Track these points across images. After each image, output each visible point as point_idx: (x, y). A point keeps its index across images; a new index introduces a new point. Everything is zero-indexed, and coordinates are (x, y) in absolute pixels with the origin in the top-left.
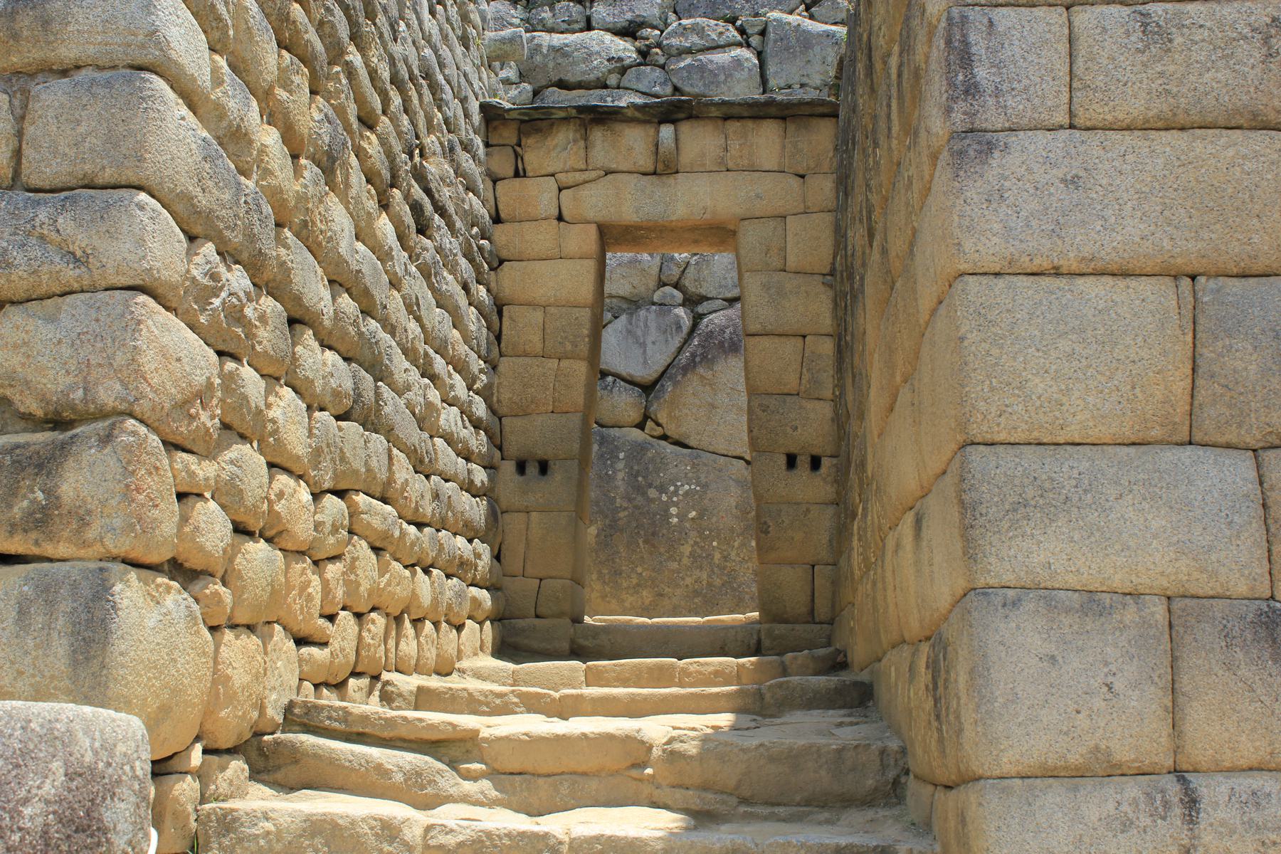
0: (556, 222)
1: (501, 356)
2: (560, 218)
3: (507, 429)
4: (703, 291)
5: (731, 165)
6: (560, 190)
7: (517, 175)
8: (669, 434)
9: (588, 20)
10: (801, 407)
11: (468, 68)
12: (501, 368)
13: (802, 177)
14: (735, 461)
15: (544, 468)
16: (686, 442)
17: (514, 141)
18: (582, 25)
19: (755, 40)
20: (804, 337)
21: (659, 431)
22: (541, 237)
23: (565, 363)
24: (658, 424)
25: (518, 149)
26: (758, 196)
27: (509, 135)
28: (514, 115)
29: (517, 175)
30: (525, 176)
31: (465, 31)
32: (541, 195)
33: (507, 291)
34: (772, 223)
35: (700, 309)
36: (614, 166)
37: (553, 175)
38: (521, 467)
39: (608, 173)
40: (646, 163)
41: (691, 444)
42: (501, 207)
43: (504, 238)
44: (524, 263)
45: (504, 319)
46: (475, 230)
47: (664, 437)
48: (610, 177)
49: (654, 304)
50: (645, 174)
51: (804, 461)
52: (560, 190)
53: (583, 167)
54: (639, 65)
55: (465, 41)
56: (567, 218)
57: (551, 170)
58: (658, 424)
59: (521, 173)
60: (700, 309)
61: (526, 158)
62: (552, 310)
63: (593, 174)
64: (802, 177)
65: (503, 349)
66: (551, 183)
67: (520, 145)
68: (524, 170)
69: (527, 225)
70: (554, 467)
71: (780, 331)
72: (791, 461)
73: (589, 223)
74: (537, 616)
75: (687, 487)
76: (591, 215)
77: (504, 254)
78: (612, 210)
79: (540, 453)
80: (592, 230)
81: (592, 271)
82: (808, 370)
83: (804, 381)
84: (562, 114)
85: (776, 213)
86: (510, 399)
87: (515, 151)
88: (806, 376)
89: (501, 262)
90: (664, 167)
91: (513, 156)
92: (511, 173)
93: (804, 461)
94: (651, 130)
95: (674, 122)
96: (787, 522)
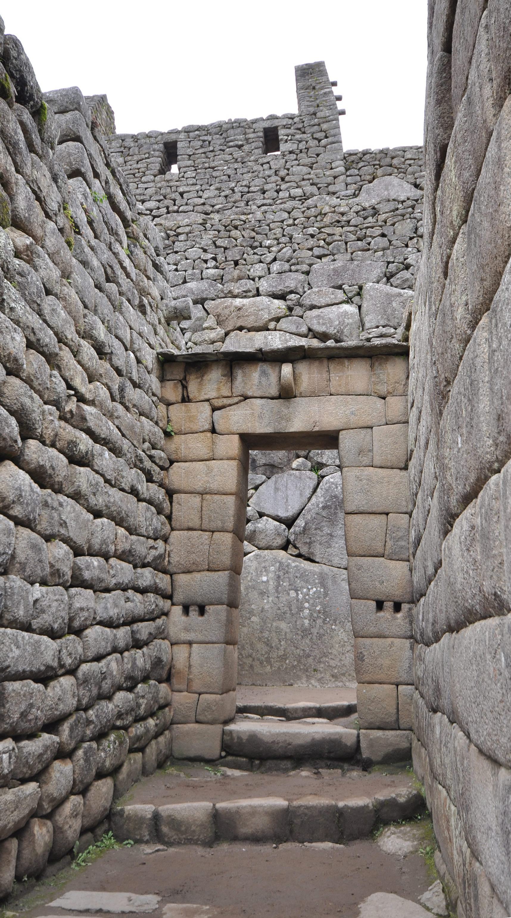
1: (172, 529)
2: (213, 431)
5: (333, 391)
9: (258, 289)
11: (146, 329)
12: (171, 540)
15: (202, 611)
18: (254, 292)
20: (387, 514)
21: (296, 552)
22: (197, 445)
25: (184, 382)
27: (177, 373)
28: (180, 359)
31: (141, 301)
32: (202, 414)
33: (176, 483)
34: (363, 431)
38: (186, 610)
39: (246, 398)
40: (274, 391)
41: (317, 560)
44: (187, 464)
45: (173, 504)
46: (147, 444)
47: (299, 556)
50: (272, 398)
51: (389, 605)
53: (230, 395)
54: (287, 316)
55: (142, 309)
56: (218, 431)
59: (186, 399)
61: (189, 389)
63: (236, 400)
64: (384, 398)
66: (206, 407)
68: (188, 397)
70: (209, 609)
71: (370, 510)
72: (380, 606)
74: (197, 722)
75: (315, 589)
76: (235, 429)
77: (173, 457)
78: (249, 425)
79: (199, 600)
80: (236, 439)
83: (387, 548)
85: (365, 425)
86: (178, 562)
89: (172, 462)
90: (286, 394)
93: (389, 605)
95: (292, 362)
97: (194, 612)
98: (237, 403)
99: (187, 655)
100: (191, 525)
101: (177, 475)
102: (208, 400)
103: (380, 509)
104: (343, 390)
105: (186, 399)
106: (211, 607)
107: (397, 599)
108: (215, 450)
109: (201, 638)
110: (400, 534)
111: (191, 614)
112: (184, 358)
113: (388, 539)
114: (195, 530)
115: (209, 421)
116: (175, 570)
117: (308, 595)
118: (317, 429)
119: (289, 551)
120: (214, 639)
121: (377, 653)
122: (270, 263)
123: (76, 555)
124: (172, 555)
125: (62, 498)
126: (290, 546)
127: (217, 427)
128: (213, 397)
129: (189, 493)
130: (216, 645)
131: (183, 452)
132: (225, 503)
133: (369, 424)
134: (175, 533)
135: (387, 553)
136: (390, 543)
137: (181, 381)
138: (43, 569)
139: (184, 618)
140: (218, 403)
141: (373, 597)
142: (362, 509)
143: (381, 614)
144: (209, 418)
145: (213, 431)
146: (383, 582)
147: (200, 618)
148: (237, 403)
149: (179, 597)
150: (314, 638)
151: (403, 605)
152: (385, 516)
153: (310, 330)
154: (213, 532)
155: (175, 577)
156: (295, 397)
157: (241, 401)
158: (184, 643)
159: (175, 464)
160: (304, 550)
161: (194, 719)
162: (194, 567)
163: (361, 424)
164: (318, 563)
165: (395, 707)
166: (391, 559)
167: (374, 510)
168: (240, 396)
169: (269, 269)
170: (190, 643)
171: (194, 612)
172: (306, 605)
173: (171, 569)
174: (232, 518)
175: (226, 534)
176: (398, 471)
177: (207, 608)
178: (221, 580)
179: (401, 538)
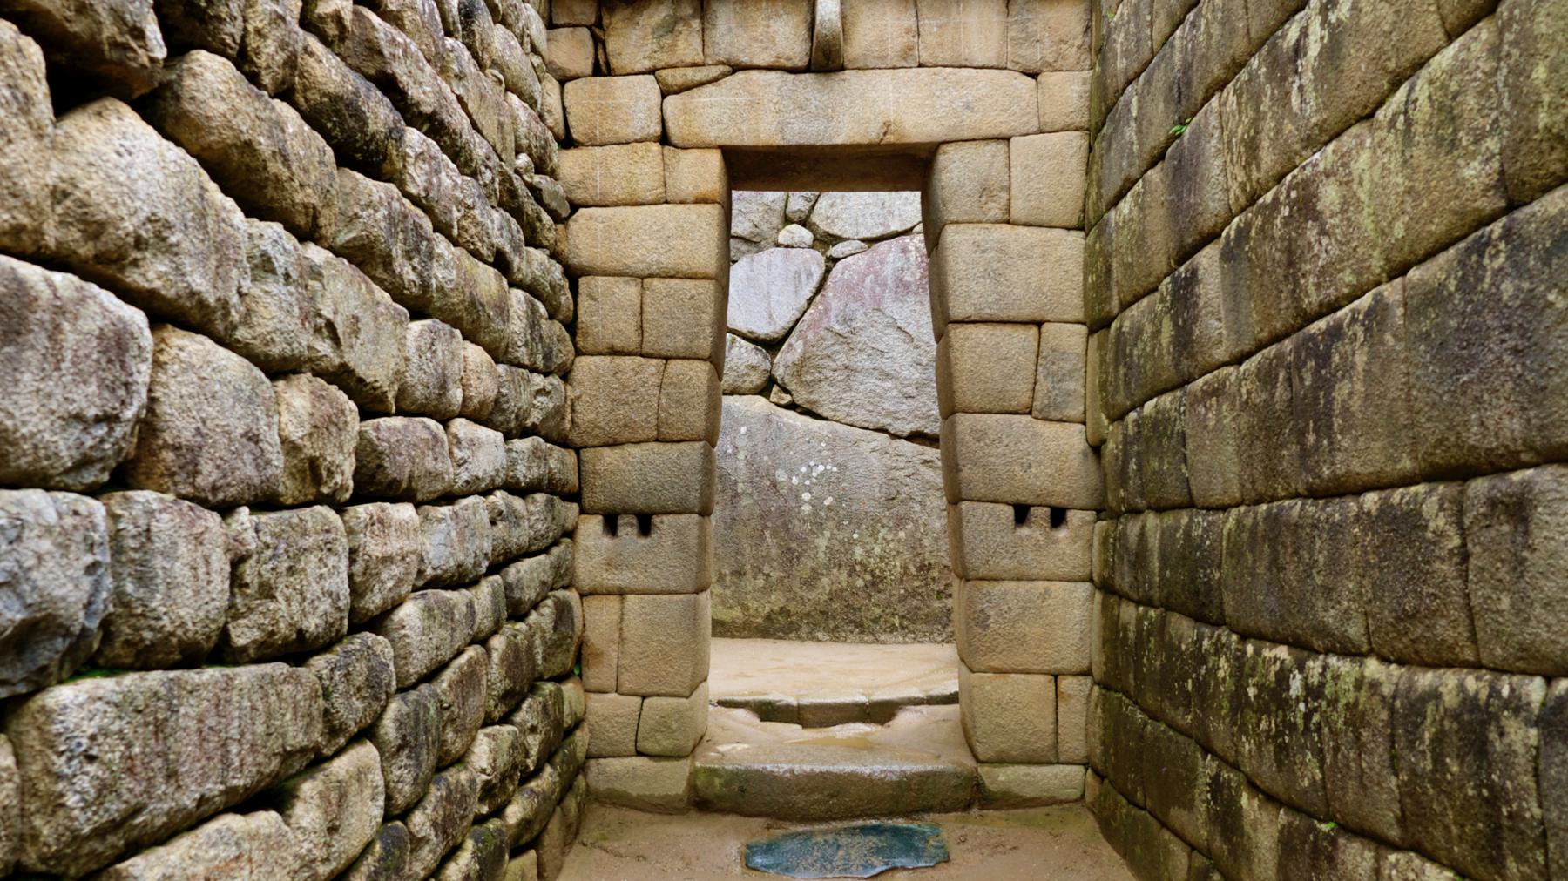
1: (579, 352)
2: (664, 139)
4: (835, 231)
6: (664, 96)
15: (645, 527)
20: (1039, 324)
21: (787, 398)
25: (597, 31)
26: (968, 107)
30: (609, 74)
36: (745, 59)
37: (652, 71)
38: (611, 526)
39: (736, 68)
42: (572, 121)
45: (581, 299)
46: (523, 159)
47: (792, 406)
48: (740, 75)
49: (778, 245)
51: (1040, 514)
52: (664, 96)
53: (699, 59)
56: (674, 139)
59: (604, 68)
60: (835, 251)
61: (610, 47)
63: (715, 71)
64: (1034, 75)
65: (580, 344)
68: (607, 63)
70: (663, 523)
71: (1004, 316)
72: (1022, 514)
73: (708, 147)
74: (639, 754)
75: (821, 468)
77: (579, 195)
78: (744, 127)
79: (639, 503)
81: (715, 223)
83: (1039, 395)
85: (995, 133)
86: (591, 421)
89: (575, 207)
91: (590, 42)
93: (1040, 514)
97: (627, 528)
98: (715, 80)
99: (616, 618)
100: (618, 343)
101: (588, 236)
103: (1026, 314)
104: (946, 56)
105: (602, 69)
106: (665, 518)
107: (1057, 501)
108: (669, 182)
109: (643, 581)
110: (1067, 366)
111: (622, 531)
113: (1040, 377)
114: (629, 354)
115: (656, 118)
117: (809, 478)
118: (890, 138)
119: (773, 398)
120: (673, 585)
121: (1016, 611)
123: (365, 415)
124: (578, 408)
125: (317, 254)
126: (775, 388)
127: (673, 130)
129: (615, 275)
130: (676, 597)
131: (600, 184)
133: (1004, 130)
134: (583, 361)
135: (1037, 405)
136: (1044, 385)
137: (589, 28)
138: (261, 462)
139: (606, 541)
140: (674, 77)
141: (1008, 498)
142: (987, 312)
143: (1024, 531)
144: (657, 111)
145: (664, 139)
147: (643, 541)
148: (715, 80)
151: (1070, 514)
152: (1034, 330)
154: (667, 359)
155: (587, 454)
156: (843, 68)
157: (724, 75)
158: (609, 593)
159: (582, 210)
160: (801, 397)
161: (632, 748)
162: (627, 435)
164: (826, 419)
166: (1046, 419)
167: (1013, 314)
168: (723, 63)
170: (622, 593)
171: (627, 528)
172: (806, 496)
173: (577, 441)
174: (708, 330)
175: (697, 363)
176: (1064, 232)
177: (656, 520)
178: (685, 462)
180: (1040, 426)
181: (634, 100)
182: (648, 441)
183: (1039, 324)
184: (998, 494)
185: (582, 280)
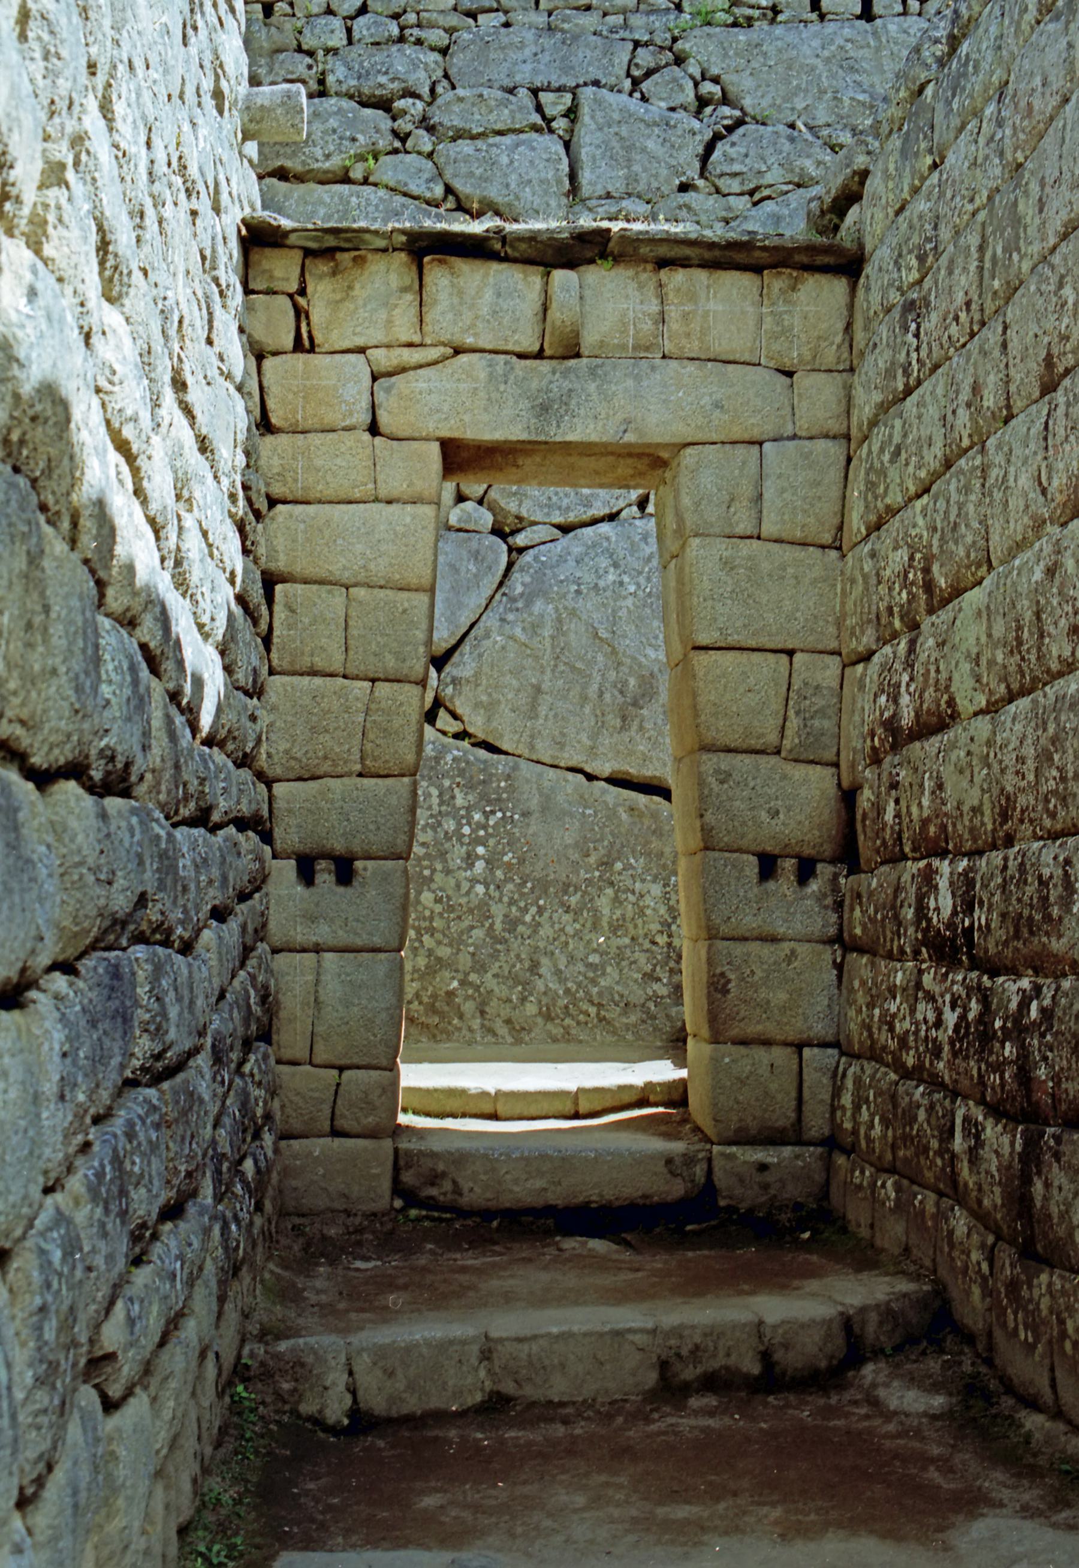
0: (367, 436)
2: (374, 429)
3: (280, 804)
6: (375, 378)
7: (298, 346)
8: (471, 730)
10: (784, 777)
13: (790, 374)
14: (570, 776)
16: (497, 744)
17: (294, 287)
19: (560, 124)
20: (790, 653)
21: (454, 727)
22: (343, 460)
23: (384, 689)
24: (455, 716)
25: (302, 301)
29: (298, 346)
30: (312, 350)
35: (520, 540)
36: (470, 341)
37: (362, 350)
41: (505, 747)
42: (271, 404)
43: (276, 461)
45: (277, 608)
48: (463, 358)
54: (396, 151)
57: (360, 341)
58: (455, 716)
59: (306, 343)
60: (520, 540)
62: (360, 593)
63: (434, 353)
64: (790, 374)
65: (275, 663)
67: (302, 292)
69: (315, 439)
72: (768, 866)
73: (427, 439)
74: (336, 1133)
79: (339, 846)
82: (797, 713)
83: (788, 733)
84: (381, 243)
86: (287, 752)
87: (295, 306)
88: (794, 722)
92: (289, 342)
94: (534, 278)
96: (759, 974)
98: (435, 363)
100: (320, 663)
102: (362, 350)
104: (693, 347)
106: (370, 864)
107: (807, 851)
109: (343, 937)
110: (820, 702)
111: (320, 878)
112: (307, 239)
113: (791, 713)
115: (364, 403)
116: (278, 771)
117: (485, 827)
120: (377, 941)
121: (759, 974)
122: (352, 18)
126: (442, 713)
128: (374, 342)
129: (315, 582)
130: (382, 956)
132: (404, 611)
133: (756, 434)
135: (787, 744)
137: (291, 296)
143: (771, 885)
145: (374, 429)
146: (777, 813)
147: (341, 890)
148: (435, 363)
149: (287, 835)
150: (498, 926)
151: (819, 867)
152: (784, 658)
153: (449, 190)
154: (373, 681)
159: (280, 507)
162: (326, 767)
163: (737, 433)
164: (506, 753)
165: (794, 1094)
166: (796, 761)
168: (445, 345)
169: (349, 31)
170: (317, 949)
172: (481, 850)
175: (407, 687)
176: (818, 552)
177: (359, 864)
179: (821, 712)
180: (789, 768)
181: (344, 384)
182: (349, 774)
183: (790, 653)
184: (744, 843)
185: (279, 588)
